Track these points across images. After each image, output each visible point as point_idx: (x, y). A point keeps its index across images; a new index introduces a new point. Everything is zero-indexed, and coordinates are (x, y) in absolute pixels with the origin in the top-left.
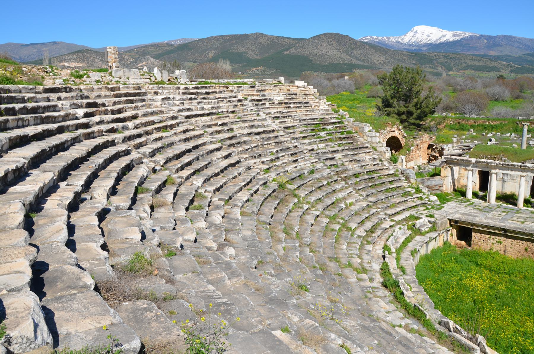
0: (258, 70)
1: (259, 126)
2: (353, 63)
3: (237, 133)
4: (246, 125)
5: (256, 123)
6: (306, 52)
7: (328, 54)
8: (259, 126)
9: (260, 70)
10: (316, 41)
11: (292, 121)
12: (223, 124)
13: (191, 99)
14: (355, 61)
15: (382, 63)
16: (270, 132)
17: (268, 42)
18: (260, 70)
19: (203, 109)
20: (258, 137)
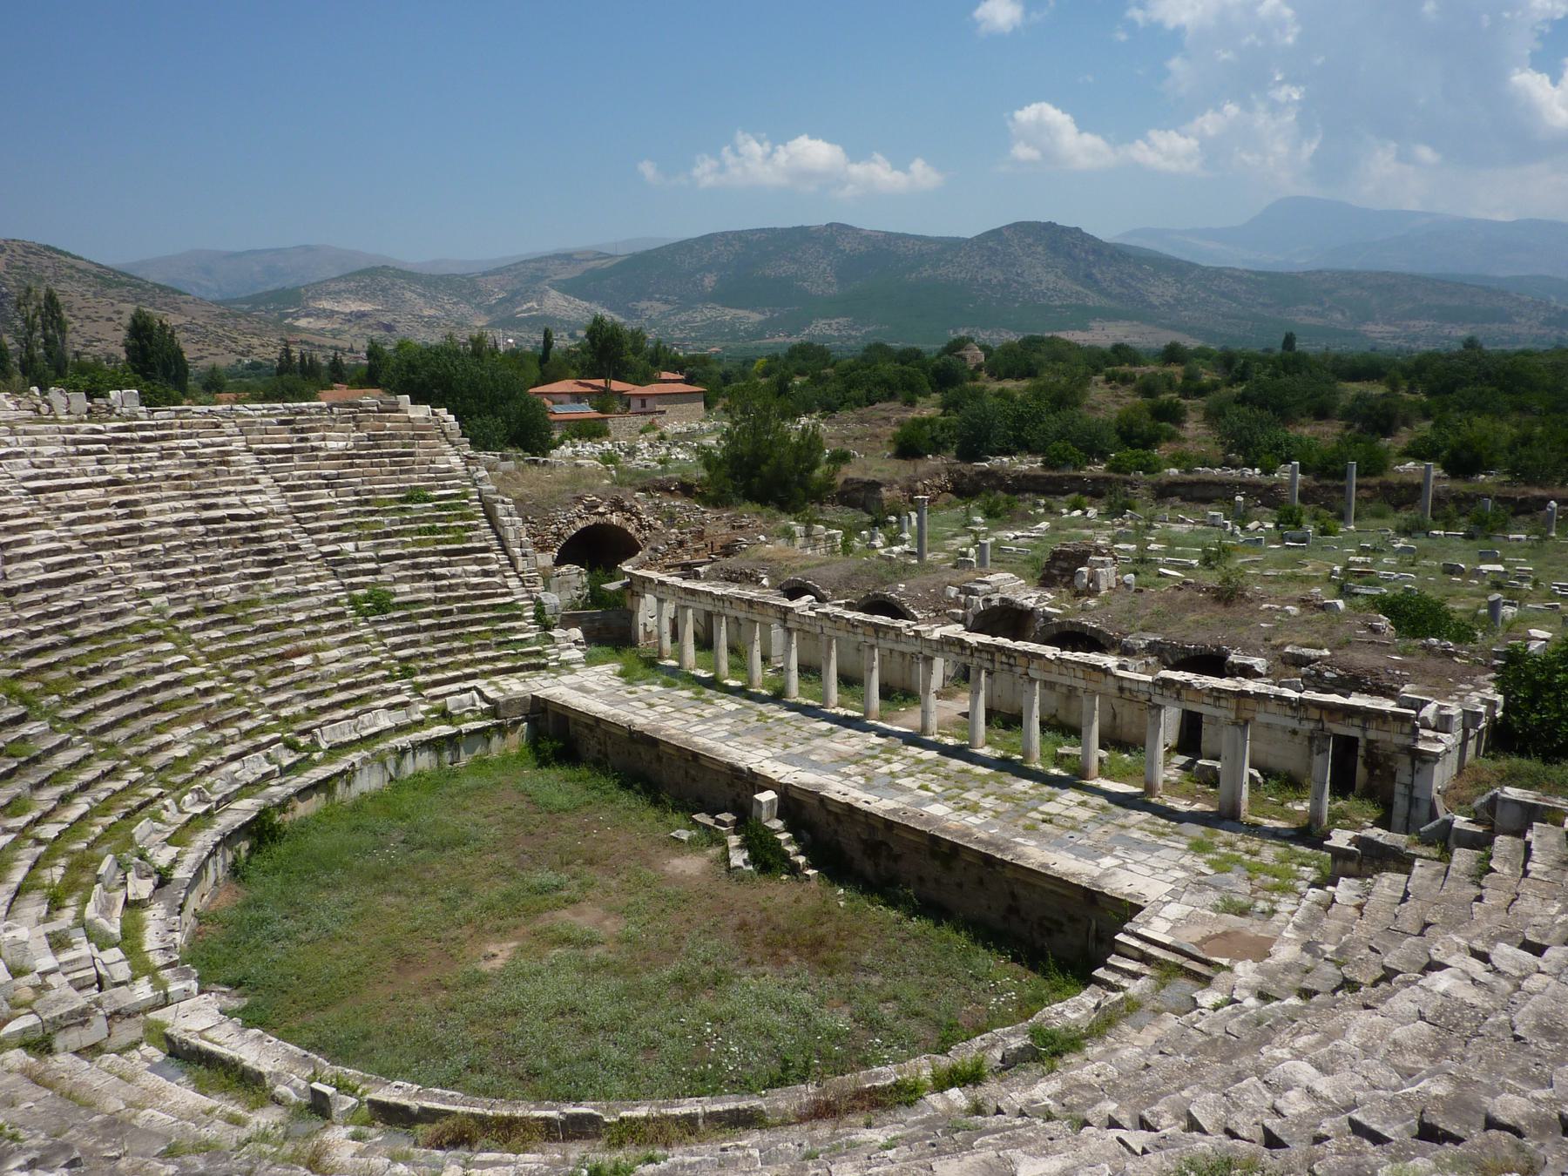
0: (830, 325)
1: (228, 506)
2: (1091, 303)
3: (146, 522)
4: (192, 503)
5: (221, 501)
6: (963, 275)
7: (1021, 280)
8: (228, 506)
9: (834, 326)
10: (990, 244)
11: (333, 493)
12: (121, 505)
13: (86, 453)
14: (1093, 299)
15: (1172, 302)
16: (251, 517)
17: (862, 248)
18: (834, 326)
19: (104, 472)
20: (200, 528)
